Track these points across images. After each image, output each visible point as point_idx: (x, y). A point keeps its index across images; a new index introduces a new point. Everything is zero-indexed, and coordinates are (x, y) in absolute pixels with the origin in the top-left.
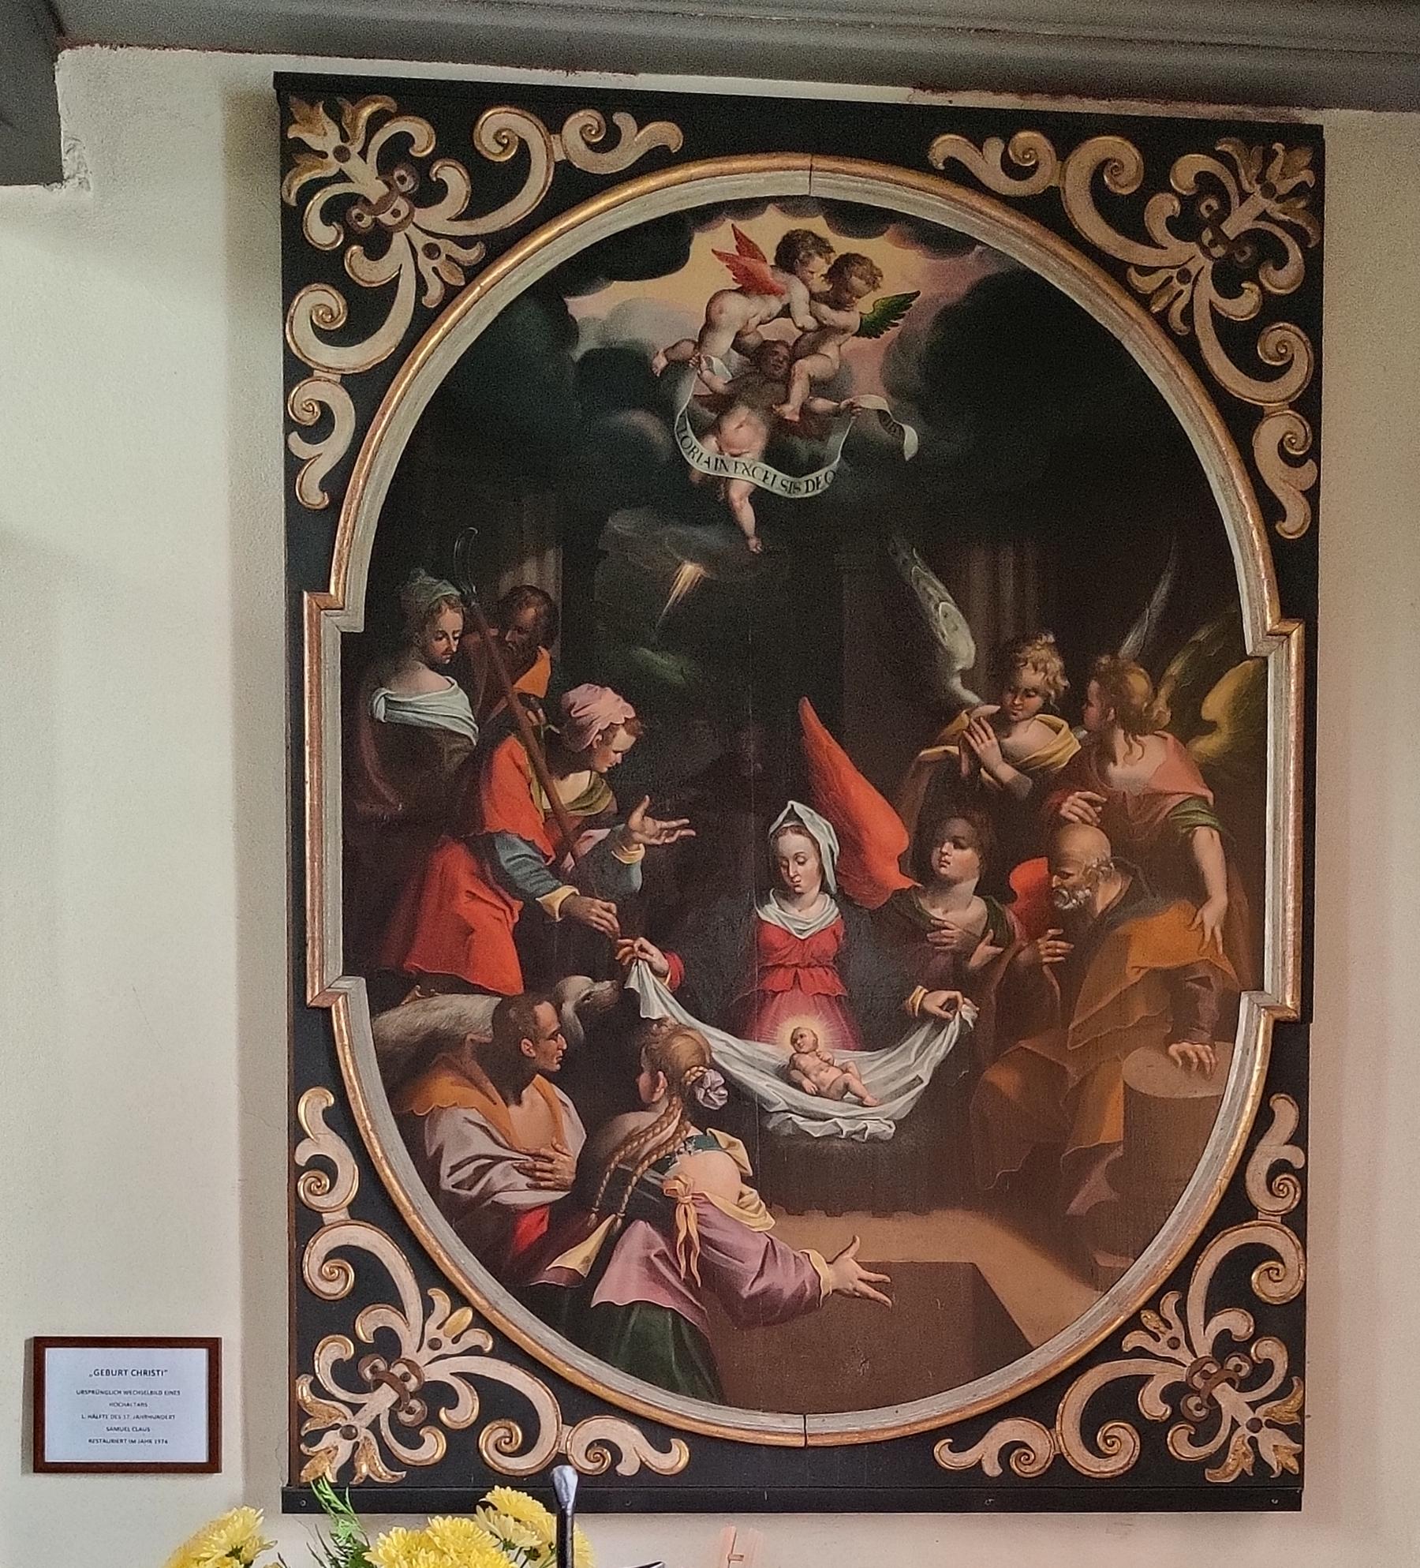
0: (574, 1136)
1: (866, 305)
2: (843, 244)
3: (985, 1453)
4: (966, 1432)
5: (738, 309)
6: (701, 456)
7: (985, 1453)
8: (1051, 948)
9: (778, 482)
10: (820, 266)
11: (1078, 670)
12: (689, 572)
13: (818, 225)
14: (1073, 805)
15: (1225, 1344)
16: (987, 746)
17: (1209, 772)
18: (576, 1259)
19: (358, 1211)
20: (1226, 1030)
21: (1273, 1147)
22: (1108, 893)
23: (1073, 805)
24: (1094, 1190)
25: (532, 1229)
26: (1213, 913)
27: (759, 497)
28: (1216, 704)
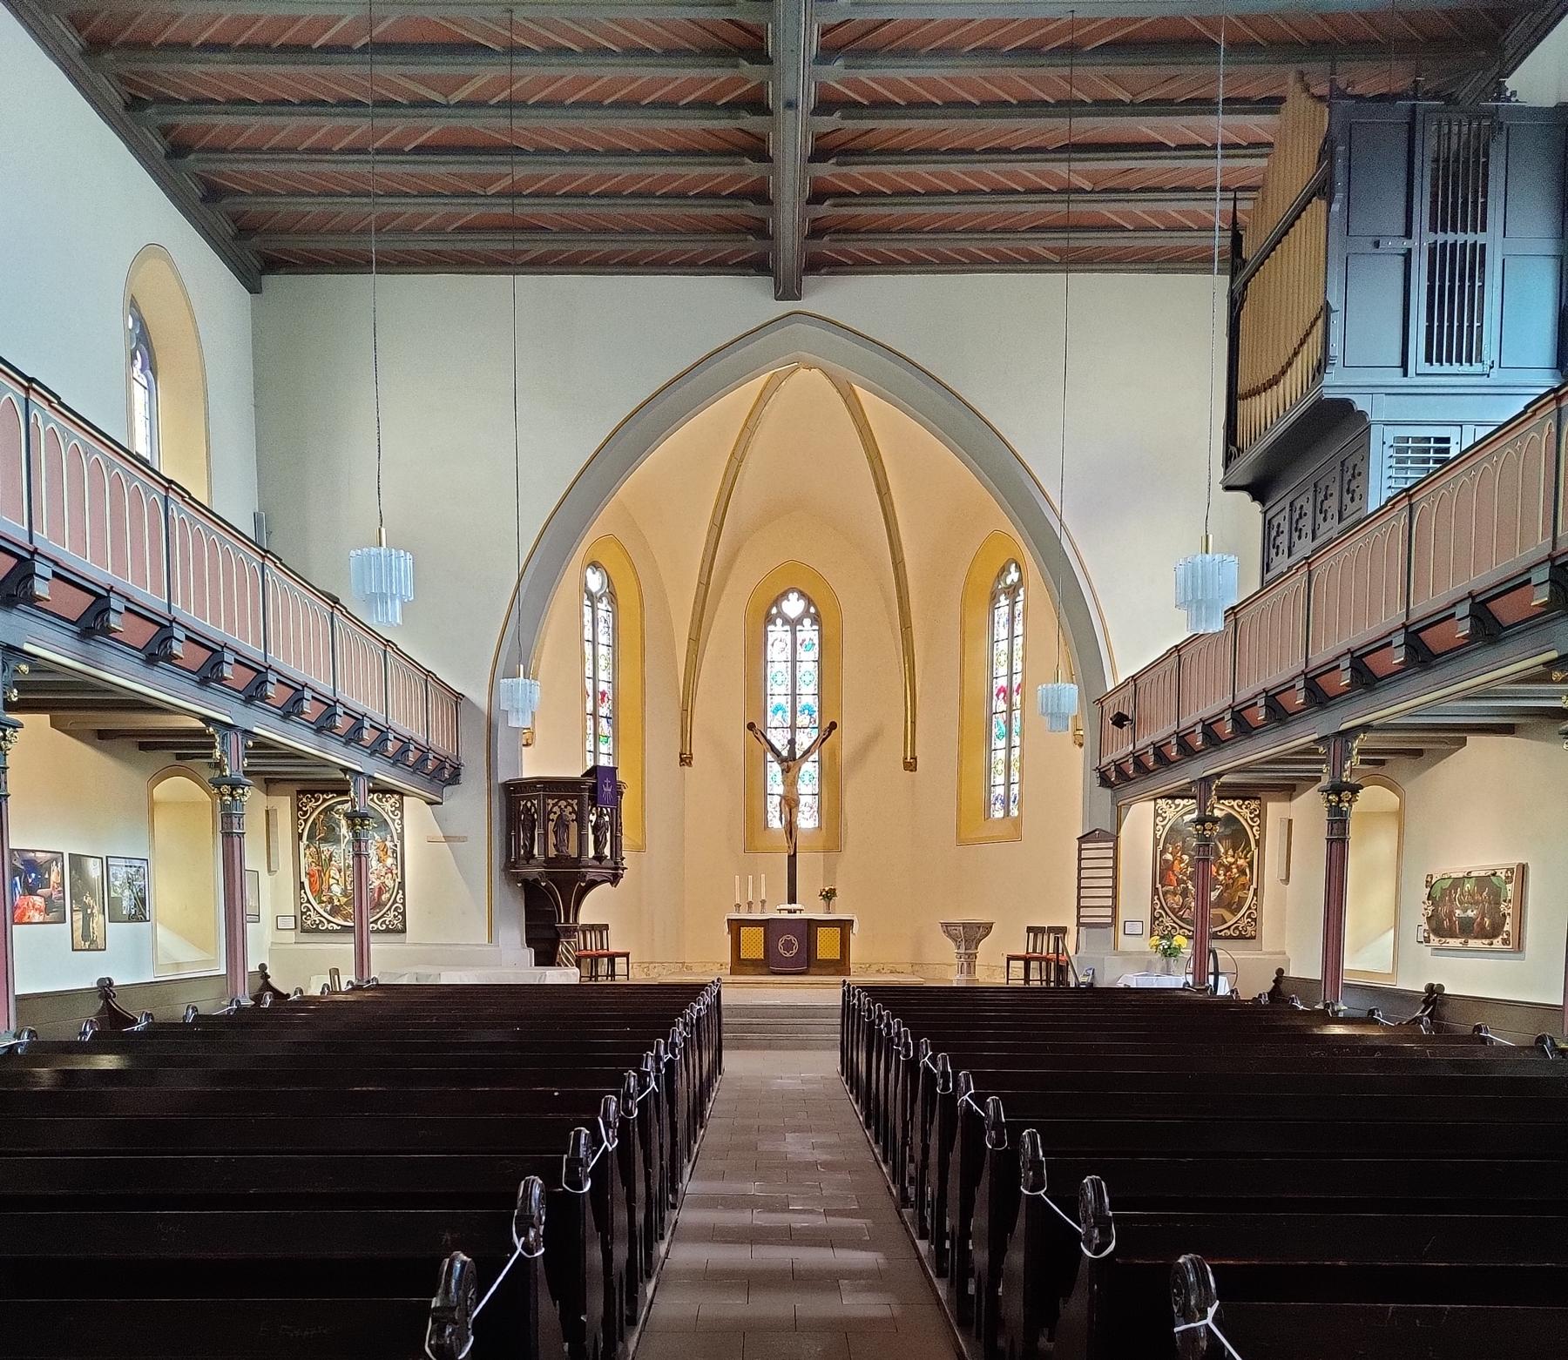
0: (1181, 901)
3: (1222, 933)
4: (1220, 931)
7: (1222, 933)
8: (1231, 881)
11: (1234, 853)
15: (1248, 922)
16: (1224, 860)
17: (1248, 863)
18: (1181, 913)
19: (1160, 908)
20: (1249, 890)
21: (1254, 902)
22: (1237, 875)
23: (1233, 866)
24: (1235, 906)
25: (1177, 910)
26: (1248, 877)
28: (1248, 856)
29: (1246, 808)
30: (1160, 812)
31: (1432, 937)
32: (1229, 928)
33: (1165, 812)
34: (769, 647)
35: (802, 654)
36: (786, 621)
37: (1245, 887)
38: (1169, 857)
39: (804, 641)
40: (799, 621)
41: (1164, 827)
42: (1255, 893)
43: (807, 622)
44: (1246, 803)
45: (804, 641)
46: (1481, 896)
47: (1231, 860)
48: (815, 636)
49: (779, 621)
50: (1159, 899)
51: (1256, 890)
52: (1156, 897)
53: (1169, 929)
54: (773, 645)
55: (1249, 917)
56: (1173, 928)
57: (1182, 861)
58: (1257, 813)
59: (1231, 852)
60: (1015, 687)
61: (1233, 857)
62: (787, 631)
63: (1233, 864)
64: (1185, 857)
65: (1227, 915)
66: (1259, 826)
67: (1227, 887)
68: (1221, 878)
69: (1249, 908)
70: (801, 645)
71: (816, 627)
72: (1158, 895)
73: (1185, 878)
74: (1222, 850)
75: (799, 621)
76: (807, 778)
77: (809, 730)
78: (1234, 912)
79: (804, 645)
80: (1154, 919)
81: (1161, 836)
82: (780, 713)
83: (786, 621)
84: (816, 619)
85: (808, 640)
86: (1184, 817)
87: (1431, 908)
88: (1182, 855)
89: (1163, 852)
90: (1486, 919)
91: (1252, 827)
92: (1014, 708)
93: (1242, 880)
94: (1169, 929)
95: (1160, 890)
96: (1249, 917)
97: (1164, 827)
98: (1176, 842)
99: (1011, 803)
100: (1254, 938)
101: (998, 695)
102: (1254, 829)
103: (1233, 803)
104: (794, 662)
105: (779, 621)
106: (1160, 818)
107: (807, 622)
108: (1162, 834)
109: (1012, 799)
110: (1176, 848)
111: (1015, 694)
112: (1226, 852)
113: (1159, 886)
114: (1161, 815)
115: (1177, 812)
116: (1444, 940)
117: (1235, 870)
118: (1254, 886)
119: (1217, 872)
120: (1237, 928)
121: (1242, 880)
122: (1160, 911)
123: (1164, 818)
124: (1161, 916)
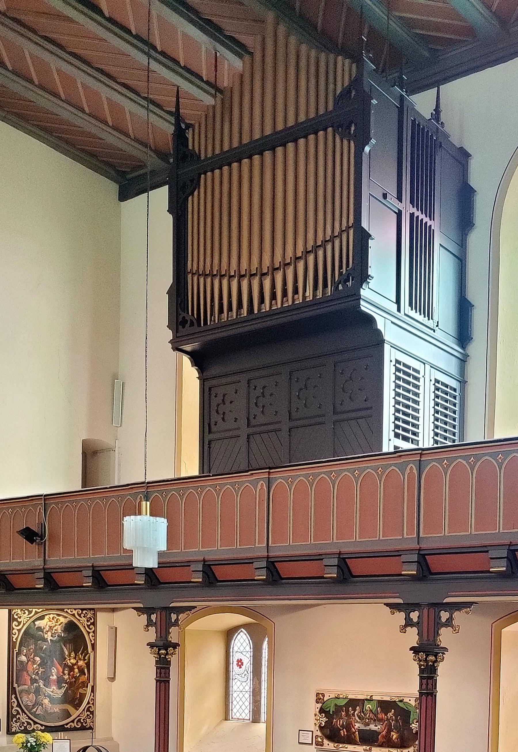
0: (35, 698)
1: (59, 623)
2: (57, 618)
3: (68, 726)
4: (67, 724)
5: (49, 623)
6: (46, 636)
7: (68, 726)
8: (74, 680)
9: (52, 638)
10: (55, 619)
11: (76, 655)
12: (45, 646)
13: (55, 616)
14: (75, 667)
15: (88, 715)
16: (68, 661)
17: (86, 664)
18: (34, 710)
20: (87, 687)
21: (92, 697)
22: (78, 675)
23: (75, 667)
24: (77, 701)
25: (31, 707)
26: (86, 676)
27: (50, 640)
28: (86, 658)
29: (84, 617)
30: (16, 617)
31: (326, 742)
32: (73, 721)
33: (20, 617)
37: (85, 685)
38: (24, 658)
41: (19, 631)
42: (93, 691)
44: (84, 612)
46: (386, 715)
47: (73, 661)
50: (16, 698)
51: (93, 687)
52: (13, 696)
53: (25, 725)
55: (88, 710)
56: (29, 723)
57: (34, 662)
58: (92, 621)
59: (73, 655)
61: (75, 658)
63: (75, 664)
64: (38, 659)
65: (71, 709)
66: (94, 632)
67: (71, 684)
68: (66, 677)
69: (88, 703)
72: (16, 694)
73: (37, 678)
74: (67, 653)
78: (77, 706)
80: (10, 716)
81: (16, 639)
86: (36, 623)
87: (325, 719)
88: (34, 656)
89: (19, 654)
90: (392, 733)
91: (89, 633)
93: (83, 678)
94: (25, 725)
95: (17, 689)
96: (88, 710)
97: (19, 631)
98: (28, 646)
100: (91, 728)
102: (91, 634)
103: (74, 612)
106: (15, 623)
108: (17, 637)
110: (29, 650)
112: (69, 655)
113: (15, 685)
114: (16, 620)
115: (30, 618)
116: (341, 746)
117: (76, 670)
118: (91, 683)
119: (63, 672)
120: (79, 721)
121: (83, 678)
122: (18, 709)
123: (19, 623)
124: (18, 713)
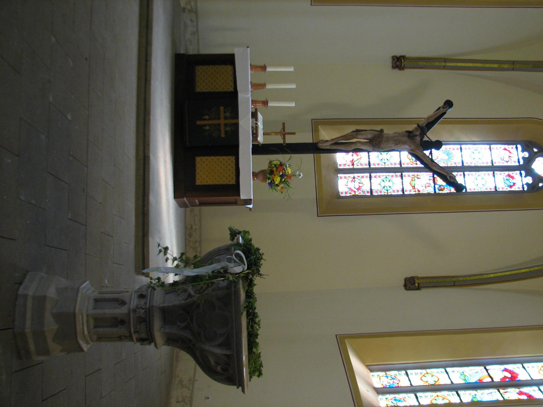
34: (503, 146)
35: (501, 176)
36: (529, 161)
39: (513, 178)
40: (529, 172)
43: (529, 180)
45: (513, 178)
48: (518, 187)
49: (526, 154)
54: (505, 149)
60: (525, 390)
62: (519, 162)
70: (509, 175)
71: (526, 189)
75: (529, 172)
76: (387, 184)
77: (433, 185)
79: (508, 178)
82: (446, 157)
83: (529, 161)
84: (533, 187)
85: (514, 181)
92: (502, 391)
99: (392, 396)
101: (506, 370)
104: (493, 168)
105: (526, 154)
107: (529, 180)
109: (397, 396)
111: (517, 390)
